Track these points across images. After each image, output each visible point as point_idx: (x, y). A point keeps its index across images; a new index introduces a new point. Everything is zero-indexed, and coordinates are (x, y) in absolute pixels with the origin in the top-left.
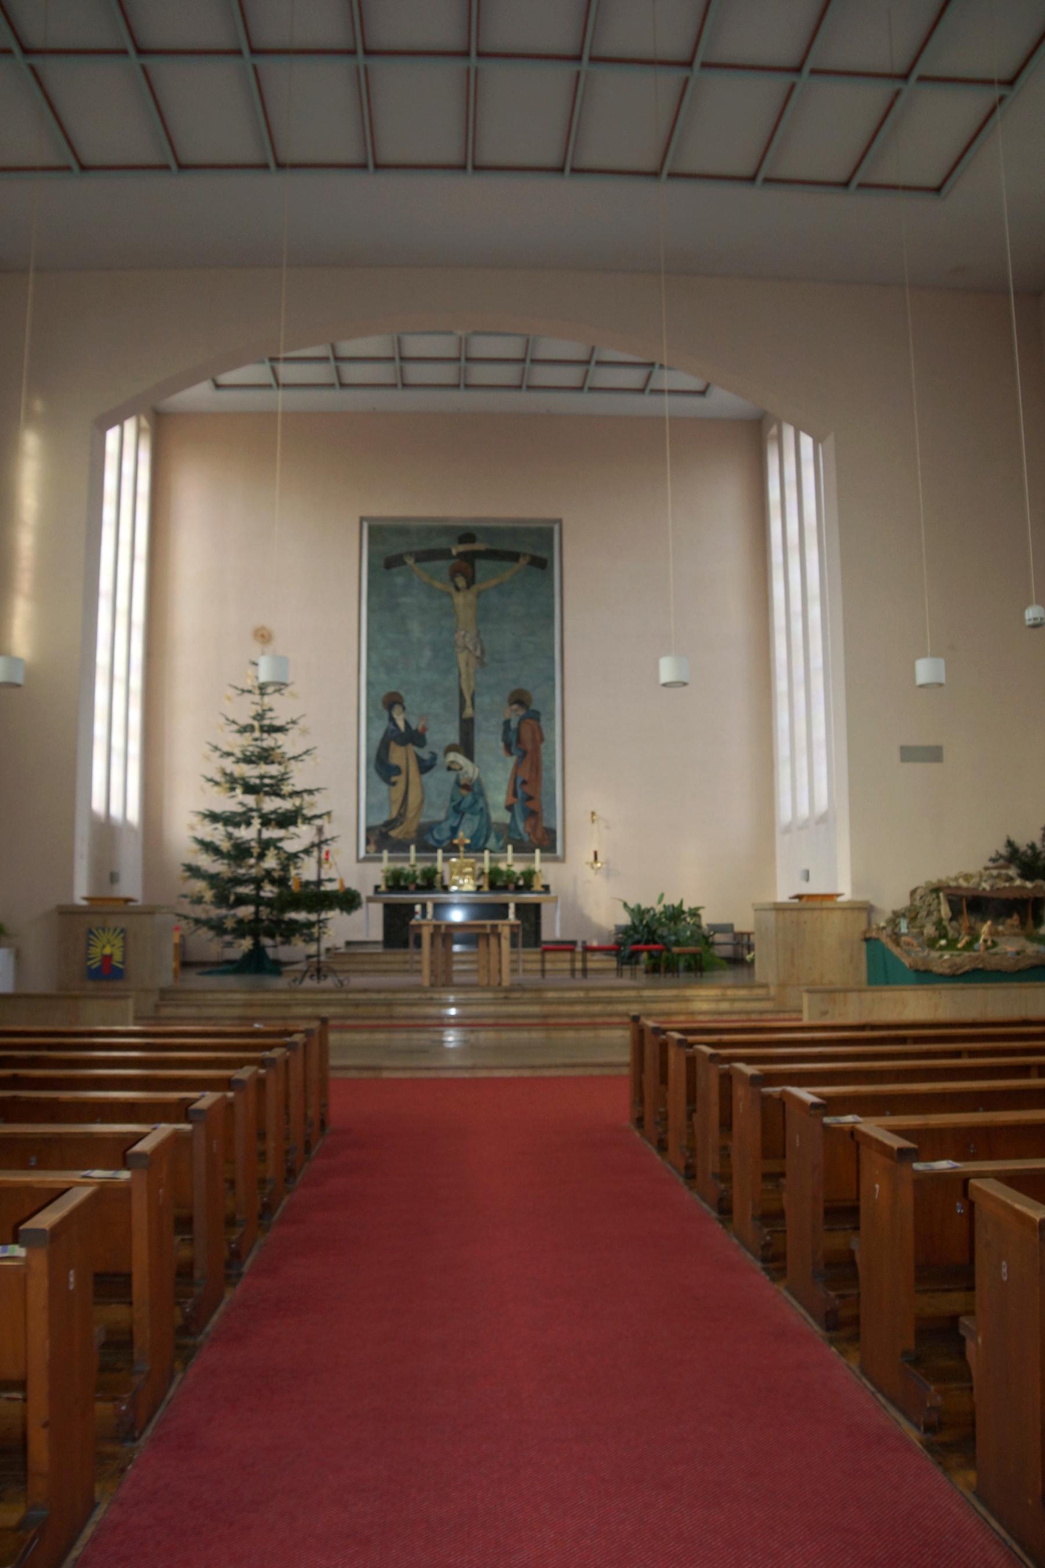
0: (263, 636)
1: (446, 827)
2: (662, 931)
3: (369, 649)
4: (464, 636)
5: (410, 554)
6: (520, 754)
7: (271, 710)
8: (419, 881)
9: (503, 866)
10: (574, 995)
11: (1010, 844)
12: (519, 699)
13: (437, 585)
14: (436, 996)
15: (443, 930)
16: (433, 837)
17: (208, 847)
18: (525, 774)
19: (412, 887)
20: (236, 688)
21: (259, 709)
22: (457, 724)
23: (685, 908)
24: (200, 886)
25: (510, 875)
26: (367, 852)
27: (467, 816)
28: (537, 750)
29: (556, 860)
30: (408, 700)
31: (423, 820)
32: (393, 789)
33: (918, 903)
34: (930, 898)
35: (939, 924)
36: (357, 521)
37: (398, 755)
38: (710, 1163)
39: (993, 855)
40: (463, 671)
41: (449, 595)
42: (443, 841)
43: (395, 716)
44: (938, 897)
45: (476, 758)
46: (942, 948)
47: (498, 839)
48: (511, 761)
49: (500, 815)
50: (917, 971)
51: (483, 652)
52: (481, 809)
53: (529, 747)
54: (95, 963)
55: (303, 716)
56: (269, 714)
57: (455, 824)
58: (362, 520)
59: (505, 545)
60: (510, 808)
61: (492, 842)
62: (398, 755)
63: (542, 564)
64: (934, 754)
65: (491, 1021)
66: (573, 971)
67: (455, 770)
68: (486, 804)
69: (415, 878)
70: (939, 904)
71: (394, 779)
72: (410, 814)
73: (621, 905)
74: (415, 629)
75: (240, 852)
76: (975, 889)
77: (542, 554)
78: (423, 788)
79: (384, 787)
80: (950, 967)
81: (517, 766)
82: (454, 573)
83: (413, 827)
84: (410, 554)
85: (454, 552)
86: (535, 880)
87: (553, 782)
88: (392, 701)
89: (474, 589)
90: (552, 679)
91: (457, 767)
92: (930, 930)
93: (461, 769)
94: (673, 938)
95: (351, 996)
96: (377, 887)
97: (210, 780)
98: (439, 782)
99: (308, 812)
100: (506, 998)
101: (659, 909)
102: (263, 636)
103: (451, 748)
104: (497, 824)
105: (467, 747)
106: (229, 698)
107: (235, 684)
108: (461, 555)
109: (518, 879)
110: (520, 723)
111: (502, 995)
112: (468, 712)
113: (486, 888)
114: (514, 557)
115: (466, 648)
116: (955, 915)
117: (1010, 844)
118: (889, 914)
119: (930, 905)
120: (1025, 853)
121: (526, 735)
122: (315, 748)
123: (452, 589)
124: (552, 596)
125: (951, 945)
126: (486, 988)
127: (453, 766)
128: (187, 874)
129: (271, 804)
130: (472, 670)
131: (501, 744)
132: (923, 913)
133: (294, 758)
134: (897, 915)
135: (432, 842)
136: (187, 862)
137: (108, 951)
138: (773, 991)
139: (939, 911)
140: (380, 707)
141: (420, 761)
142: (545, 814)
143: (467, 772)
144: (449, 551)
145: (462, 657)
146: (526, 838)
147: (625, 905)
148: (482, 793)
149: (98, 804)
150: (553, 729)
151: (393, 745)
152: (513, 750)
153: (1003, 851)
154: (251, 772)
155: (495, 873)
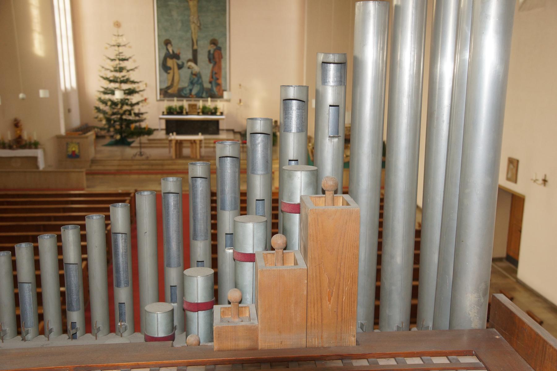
0: (118, 25)
1: (188, 89)
3: (158, 22)
12: (214, 42)
19: (175, 113)
21: (117, 52)
24: (101, 116)
27: (196, 85)
28: (220, 61)
37: (170, 63)
47: (207, 93)
48: (211, 65)
51: (200, 24)
53: (217, 60)
54: (70, 153)
56: (121, 54)
60: (211, 82)
61: (204, 95)
62: (170, 63)
68: (202, 81)
71: (169, 71)
72: (175, 84)
74: (175, 14)
78: (179, 75)
79: (165, 74)
81: (213, 67)
88: (167, 43)
90: (225, 35)
93: (193, 68)
95: (152, 162)
96: (163, 112)
99: (137, 90)
103: (189, 61)
105: (195, 60)
106: (106, 48)
112: (195, 47)
115: (194, 22)
121: (216, 56)
127: (191, 67)
131: (207, 59)
133: (132, 70)
135: (183, 94)
137: (74, 149)
140: (163, 44)
141: (178, 65)
145: (193, 26)
149: (63, 87)
155: (204, 108)
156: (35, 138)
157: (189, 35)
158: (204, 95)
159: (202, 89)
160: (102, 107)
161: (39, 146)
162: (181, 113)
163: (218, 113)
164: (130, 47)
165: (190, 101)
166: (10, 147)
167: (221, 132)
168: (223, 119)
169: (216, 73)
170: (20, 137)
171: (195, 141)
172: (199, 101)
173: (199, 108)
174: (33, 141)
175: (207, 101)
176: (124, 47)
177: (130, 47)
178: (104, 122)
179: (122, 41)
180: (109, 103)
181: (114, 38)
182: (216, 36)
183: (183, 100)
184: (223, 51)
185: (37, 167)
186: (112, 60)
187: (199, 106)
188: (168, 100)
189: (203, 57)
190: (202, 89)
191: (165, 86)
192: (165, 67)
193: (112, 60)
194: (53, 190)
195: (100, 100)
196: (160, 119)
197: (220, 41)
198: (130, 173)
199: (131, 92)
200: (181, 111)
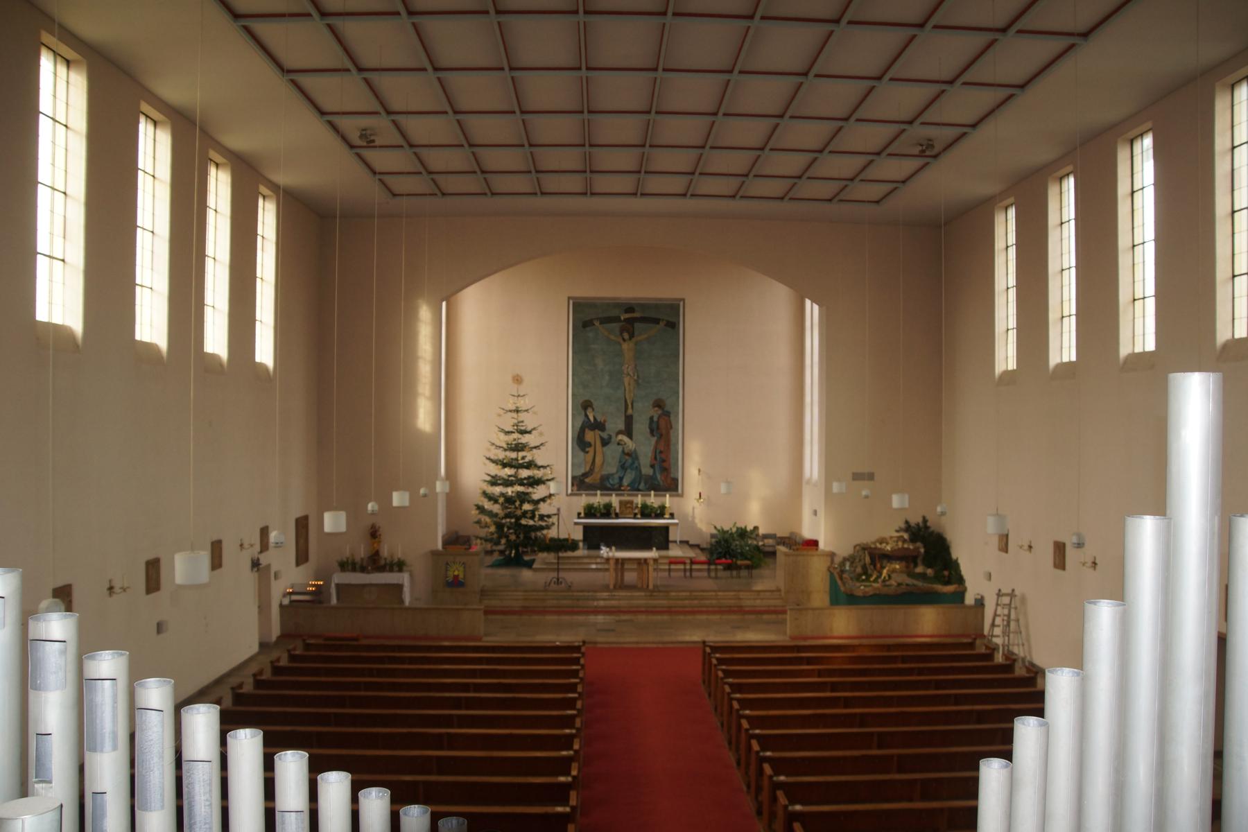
0: (518, 380)
1: (616, 476)
3: (573, 375)
4: (628, 368)
5: (597, 319)
8: (603, 511)
9: (649, 504)
10: (684, 594)
11: (907, 522)
12: (659, 404)
13: (612, 337)
16: (609, 481)
19: (598, 515)
20: (503, 409)
21: (516, 421)
22: (623, 419)
23: (748, 529)
25: (652, 508)
26: (572, 490)
27: (629, 471)
28: (668, 434)
29: (678, 496)
30: (595, 404)
31: (603, 473)
32: (587, 455)
33: (856, 554)
35: (864, 567)
36: (566, 299)
37: (590, 436)
40: (627, 389)
41: (619, 343)
43: (588, 414)
45: (634, 437)
46: (863, 581)
47: (646, 484)
48: (654, 440)
49: (647, 471)
51: (638, 377)
52: (637, 467)
53: (664, 432)
54: (450, 579)
55: (541, 425)
57: (622, 475)
58: (569, 298)
59: (653, 315)
60: (652, 466)
61: (642, 486)
62: (590, 436)
63: (673, 325)
64: (871, 477)
66: (685, 576)
67: (622, 445)
68: (639, 465)
69: (600, 509)
70: (865, 556)
71: (587, 449)
72: (597, 470)
73: (713, 527)
74: (599, 363)
75: (509, 500)
76: (883, 549)
77: (672, 320)
79: (582, 454)
81: (657, 442)
82: (622, 331)
83: (599, 476)
84: (597, 319)
85: (622, 318)
86: (666, 509)
87: (677, 453)
88: (586, 405)
89: (634, 340)
90: (678, 393)
91: (623, 443)
92: (859, 570)
93: (625, 444)
94: (739, 551)
95: (575, 594)
97: (489, 459)
98: (613, 452)
100: (651, 596)
101: (734, 530)
102: (517, 380)
103: (620, 432)
105: (628, 432)
106: (500, 415)
107: (502, 407)
108: (626, 320)
109: (657, 510)
110: (658, 419)
111: (648, 594)
112: (630, 411)
113: (639, 516)
114: (656, 321)
115: (629, 374)
116: (873, 562)
117: (907, 522)
119: (861, 556)
120: (914, 527)
121: (662, 424)
122: (546, 442)
123: (622, 341)
124: (679, 345)
125: (867, 580)
129: (524, 473)
131: (648, 430)
132: (857, 560)
133: (535, 447)
134: (845, 559)
135: (609, 485)
136: (476, 503)
137: (456, 573)
138: (783, 594)
139: (865, 559)
140: (580, 407)
141: (602, 439)
142: (672, 470)
143: (628, 446)
144: (620, 317)
145: (626, 380)
146: (661, 483)
148: (637, 458)
152: (655, 433)
153: (903, 526)
155: (645, 506)
156: (399, 554)
158: (642, 486)
160: (488, 505)
161: (405, 568)
163: (667, 516)
164: (535, 413)
165: (622, 495)
166: (363, 569)
167: (671, 545)
168: (676, 524)
169: (661, 452)
170: (377, 553)
171: (646, 560)
172: (637, 495)
173: (637, 507)
174: (396, 560)
175: (650, 495)
176: (526, 413)
177: (535, 413)
178: (493, 529)
179: (522, 404)
180: (501, 500)
181: (512, 400)
184: (672, 418)
185: (402, 601)
186: (508, 433)
187: (637, 504)
188: (587, 495)
189: (641, 427)
190: (640, 477)
192: (581, 442)
193: (508, 433)
195: (485, 494)
196: (576, 524)
198: (544, 612)
199: (535, 482)
200: (607, 511)
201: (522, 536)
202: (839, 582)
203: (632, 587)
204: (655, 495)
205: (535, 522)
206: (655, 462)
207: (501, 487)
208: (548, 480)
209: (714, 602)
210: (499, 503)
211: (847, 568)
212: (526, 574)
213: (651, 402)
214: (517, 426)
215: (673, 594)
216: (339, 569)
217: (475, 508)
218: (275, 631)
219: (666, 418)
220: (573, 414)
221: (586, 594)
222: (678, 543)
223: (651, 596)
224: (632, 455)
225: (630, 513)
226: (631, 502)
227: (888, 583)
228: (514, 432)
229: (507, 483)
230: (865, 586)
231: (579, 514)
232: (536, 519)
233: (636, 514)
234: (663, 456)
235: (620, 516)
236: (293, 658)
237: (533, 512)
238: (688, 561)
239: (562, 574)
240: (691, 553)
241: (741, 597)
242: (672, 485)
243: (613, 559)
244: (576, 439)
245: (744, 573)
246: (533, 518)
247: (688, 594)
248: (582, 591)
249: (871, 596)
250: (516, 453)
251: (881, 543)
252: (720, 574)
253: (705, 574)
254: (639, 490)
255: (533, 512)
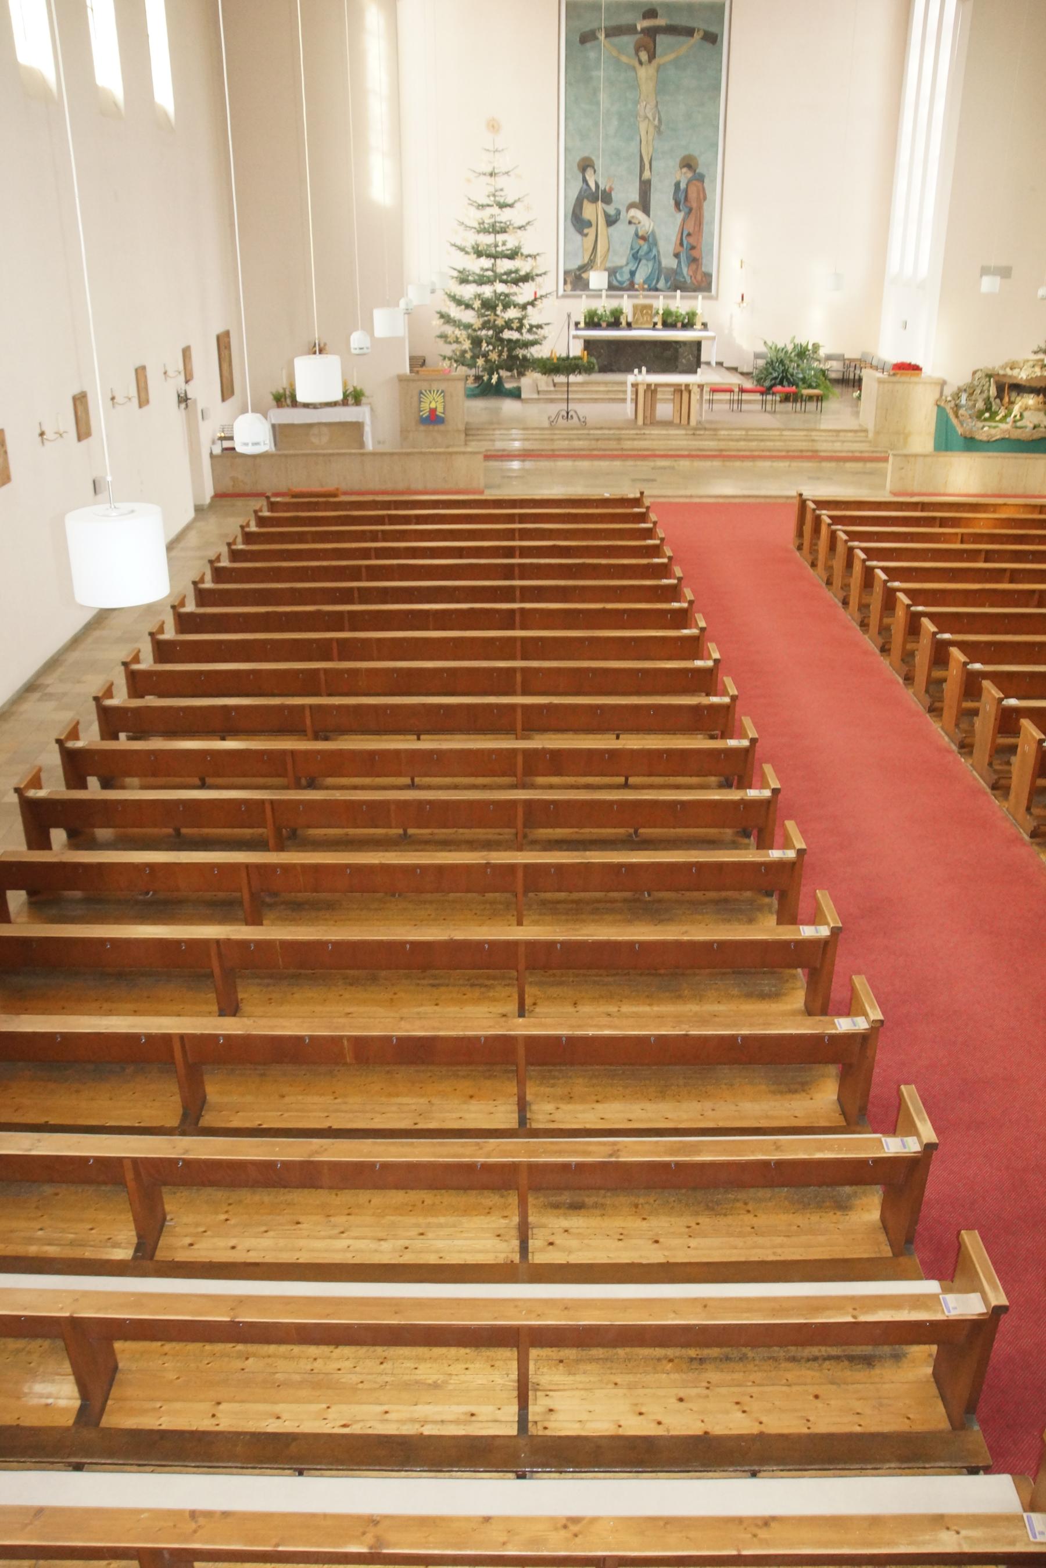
0: (494, 126)
2: (792, 367)
3: (566, 118)
6: (687, 210)
7: (502, 190)
9: (673, 309)
10: (739, 433)
12: (688, 164)
14: (647, 432)
15: (653, 387)
17: (459, 302)
18: (690, 227)
19: (604, 325)
26: (565, 291)
27: (643, 262)
28: (700, 208)
29: (711, 298)
30: (599, 164)
33: (976, 383)
34: (984, 381)
37: (589, 211)
38: (837, 581)
39: (1036, 349)
42: (624, 282)
44: (990, 381)
46: (985, 420)
47: (667, 281)
48: (680, 216)
49: (669, 262)
50: (965, 438)
52: (655, 256)
53: (694, 205)
54: (425, 414)
55: (527, 195)
57: (634, 269)
60: (677, 255)
61: (661, 284)
62: (589, 211)
65: (686, 453)
68: (658, 252)
70: (990, 385)
71: (586, 231)
72: (599, 260)
76: (1015, 378)
79: (579, 237)
80: (988, 436)
81: (684, 221)
88: (586, 165)
90: (717, 145)
92: (980, 405)
94: (801, 376)
95: (592, 432)
97: (454, 245)
98: (622, 234)
100: (694, 434)
101: (790, 348)
102: (493, 126)
103: (632, 206)
104: (667, 269)
105: (644, 205)
109: (684, 318)
110: (687, 185)
111: (691, 432)
112: (647, 174)
113: (659, 326)
115: (646, 117)
116: (1000, 396)
118: (955, 389)
121: (693, 195)
125: (992, 418)
126: (679, 426)
127: (633, 221)
128: (442, 321)
129: (504, 265)
130: (650, 138)
131: (672, 202)
132: (978, 391)
133: (520, 228)
134: (960, 390)
137: (433, 405)
138: (871, 435)
139: (989, 391)
141: (607, 216)
142: (704, 261)
143: (644, 226)
145: (643, 126)
146: (689, 281)
147: (765, 343)
148: (655, 244)
150: (714, 190)
151: (585, 202)
154: (487, 240)
155: (667, 313)
157: (633, 148)
158: (661, 284)
159: (658, 270)
160: (456, 312)
161: (364, 400)
162: (615, 324)
163: (698, 326)
165: (636, 297)
168: (707, 338)
172: (658, 297)
175: (675, 297)
176: (506, 175)
178: (467, 345)
179: (501, 163)
180: (477, 304)
182: (695, 149)
183: (622, 297)
185: (362, 444)
186: (481, 207)
189: (662, 198)
190: (658, 270)
191: (574, 265)
192: (579, 222)
193: (481, 207)
194: (402, 493)
197: (702, 161)
198: (553, 455)
201: (505, 355)
202: (954, 421)
203: (667, 424)
204: (682, 297)
205: (522, 334)
206: (679, 249)
207: (474, 285)
208: (537, 275)
209: (779, 445)
210: (473, 309)
211: (963, 402)
212: (509, 407)
213: (678, 160)
214: (494, 195)
215: (723, 432)
216: (274, 403)
217: (438, 315)
218: (209, 492)
219: (699, 184)
220: (566, 179)
221: (607, 432)
222: (714, 364)
223: (694, 434)
224: (648, 239)
225: (647, 322)
226: (650, 307)
227: (1019, 424)
228: (492, 206)
229: (481, 281)
230: (989, 427)
231: (577, 324)
232: (524, 331)
233: (655, 324)
234: (692, 240)
235: (633, 326)
236: (261, 521)
237: (520, 320)
238: (736, 390)
239: (572, 406)
240: (734, 380)
241: (816, 438)
242: (703, 284)
243: (643, 384)
244: (570, 215)
245: (811, 406)
246: (519, 329)
247: (744, 433)
248: (601, 428)
249: (996, 440)
250: (492, 235)
251: (1011, 369)
252: (780, 407)
253: (758, 407)
254: (657, 290)
255: (520, 320)
